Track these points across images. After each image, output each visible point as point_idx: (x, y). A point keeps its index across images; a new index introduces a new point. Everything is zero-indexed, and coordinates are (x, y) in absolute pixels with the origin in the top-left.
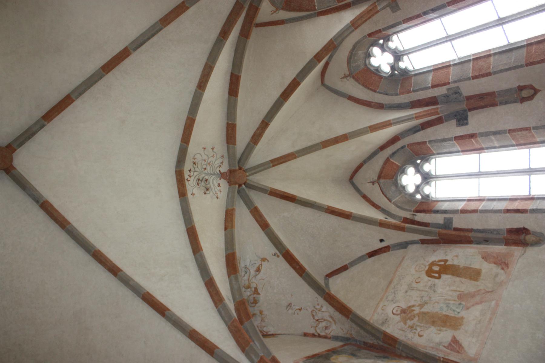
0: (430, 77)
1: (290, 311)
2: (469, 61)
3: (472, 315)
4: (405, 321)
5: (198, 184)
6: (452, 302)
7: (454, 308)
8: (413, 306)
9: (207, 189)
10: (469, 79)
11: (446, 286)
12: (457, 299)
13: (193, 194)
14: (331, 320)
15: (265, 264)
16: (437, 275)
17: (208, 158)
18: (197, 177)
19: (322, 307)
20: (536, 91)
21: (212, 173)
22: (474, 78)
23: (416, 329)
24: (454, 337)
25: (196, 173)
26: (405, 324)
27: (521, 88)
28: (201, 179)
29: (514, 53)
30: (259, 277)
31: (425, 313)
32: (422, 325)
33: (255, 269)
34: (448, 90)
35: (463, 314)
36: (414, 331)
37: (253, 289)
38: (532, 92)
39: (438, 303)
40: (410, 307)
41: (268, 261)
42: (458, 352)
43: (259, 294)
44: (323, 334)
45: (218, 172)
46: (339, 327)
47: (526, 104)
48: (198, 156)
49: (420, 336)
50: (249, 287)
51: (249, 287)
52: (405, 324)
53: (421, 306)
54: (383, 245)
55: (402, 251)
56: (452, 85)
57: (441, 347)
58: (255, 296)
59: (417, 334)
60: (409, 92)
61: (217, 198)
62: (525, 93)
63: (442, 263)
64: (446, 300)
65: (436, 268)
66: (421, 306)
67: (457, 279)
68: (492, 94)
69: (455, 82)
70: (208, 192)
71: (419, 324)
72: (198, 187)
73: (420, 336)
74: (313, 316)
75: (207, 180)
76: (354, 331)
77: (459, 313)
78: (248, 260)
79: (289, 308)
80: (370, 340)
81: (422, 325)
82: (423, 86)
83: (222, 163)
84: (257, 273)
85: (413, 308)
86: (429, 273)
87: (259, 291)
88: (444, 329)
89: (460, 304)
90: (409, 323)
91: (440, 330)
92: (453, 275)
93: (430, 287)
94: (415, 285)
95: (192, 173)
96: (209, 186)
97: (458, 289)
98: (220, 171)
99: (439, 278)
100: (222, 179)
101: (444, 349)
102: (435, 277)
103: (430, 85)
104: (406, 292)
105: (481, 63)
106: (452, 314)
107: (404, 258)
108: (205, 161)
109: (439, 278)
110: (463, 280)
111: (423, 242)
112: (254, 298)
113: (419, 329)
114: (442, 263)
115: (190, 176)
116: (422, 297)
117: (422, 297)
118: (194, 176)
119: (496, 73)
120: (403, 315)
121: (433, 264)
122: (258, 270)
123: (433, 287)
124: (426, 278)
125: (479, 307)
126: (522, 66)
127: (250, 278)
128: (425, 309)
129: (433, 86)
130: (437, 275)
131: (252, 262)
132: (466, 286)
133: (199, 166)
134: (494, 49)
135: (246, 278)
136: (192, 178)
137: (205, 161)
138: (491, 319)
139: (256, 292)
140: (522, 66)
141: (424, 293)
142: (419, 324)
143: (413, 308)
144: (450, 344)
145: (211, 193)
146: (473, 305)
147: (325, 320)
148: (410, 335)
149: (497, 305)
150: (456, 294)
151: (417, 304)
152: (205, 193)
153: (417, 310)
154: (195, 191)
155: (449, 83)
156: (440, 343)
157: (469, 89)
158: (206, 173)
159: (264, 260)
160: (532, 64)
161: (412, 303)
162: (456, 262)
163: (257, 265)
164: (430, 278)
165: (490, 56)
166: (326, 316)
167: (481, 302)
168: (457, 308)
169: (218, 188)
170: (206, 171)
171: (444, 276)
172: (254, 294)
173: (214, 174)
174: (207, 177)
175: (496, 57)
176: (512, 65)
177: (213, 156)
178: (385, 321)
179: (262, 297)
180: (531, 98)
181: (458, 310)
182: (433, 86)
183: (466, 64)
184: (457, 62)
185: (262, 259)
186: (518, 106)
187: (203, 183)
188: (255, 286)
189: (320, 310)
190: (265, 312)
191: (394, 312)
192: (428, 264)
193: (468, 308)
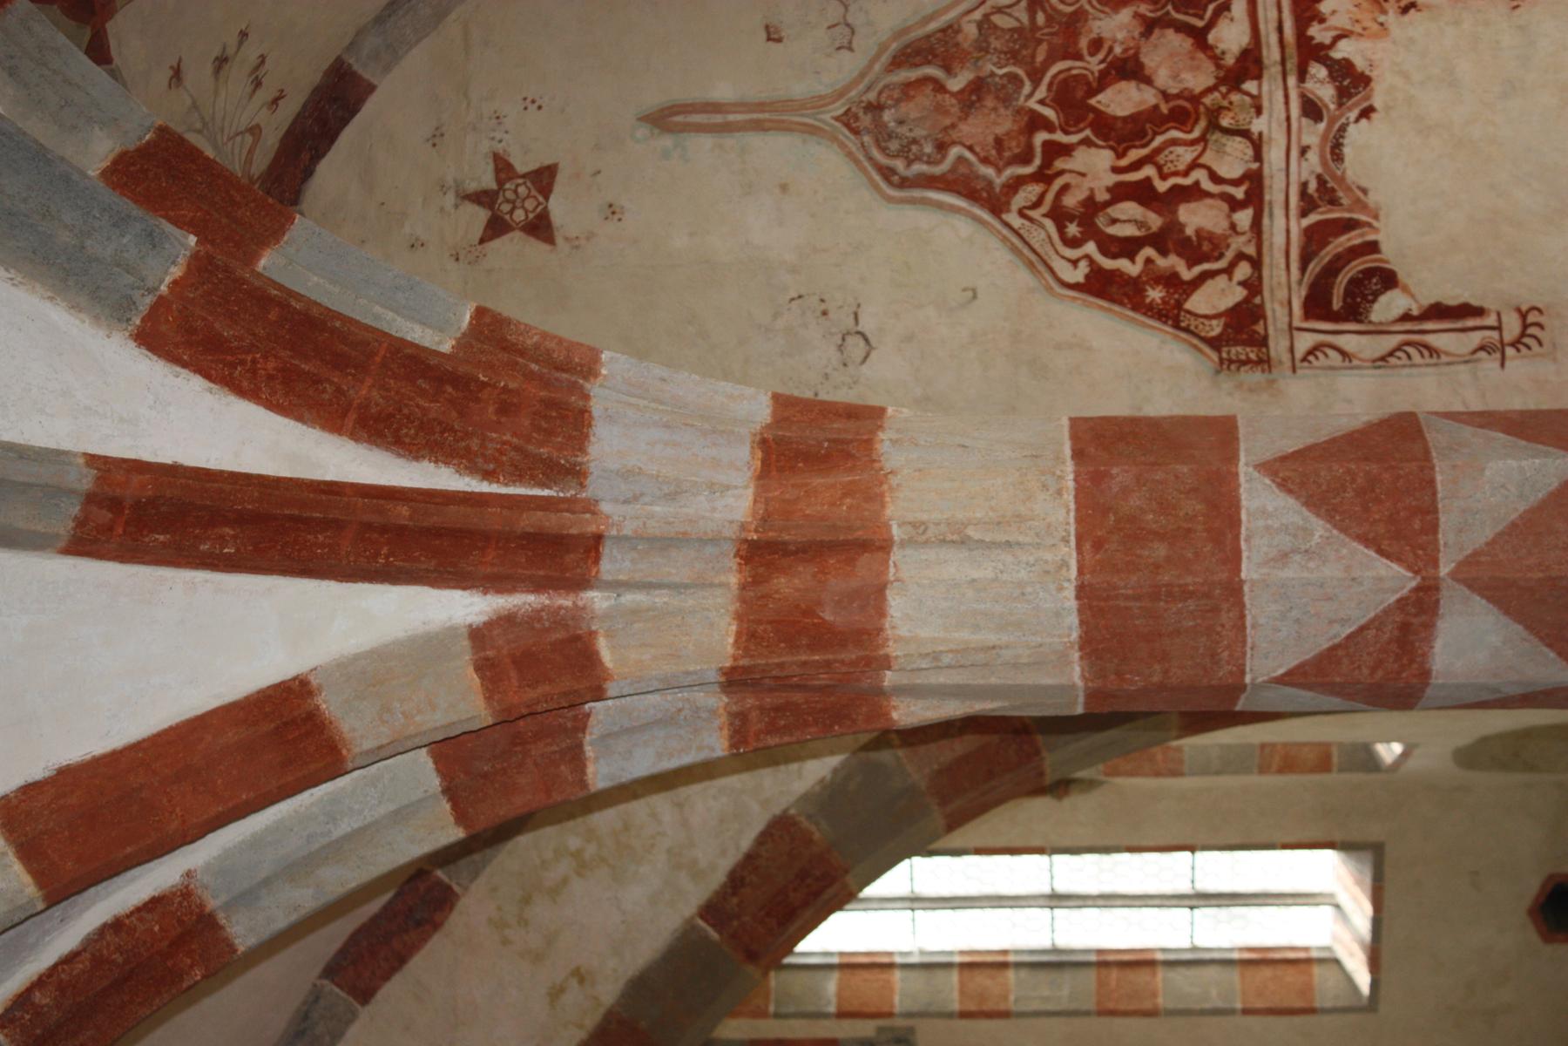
0: (831, 985)
2: (948, 966)
10: (950, 1015)
22: (964, 1015)
29: (1067, 977)
34: (880, 1030)
56: (899, 1022)
60: (761, 1014)
69: (909, 1015)
82: (811, 1008)
103: (832, 1009)
105: (981, 979)
126: (1087, 1013)
129: (842, 1015)
134: (1017, 952)
140: (1087, 1013)
155: (890, 1015)
160: (1113, 1013)
165: (1004, 965)
175: (1023, 973)
176: (1065, 1005)
182: (842, 1015)
183: (940, 974)
184: (915, 959)
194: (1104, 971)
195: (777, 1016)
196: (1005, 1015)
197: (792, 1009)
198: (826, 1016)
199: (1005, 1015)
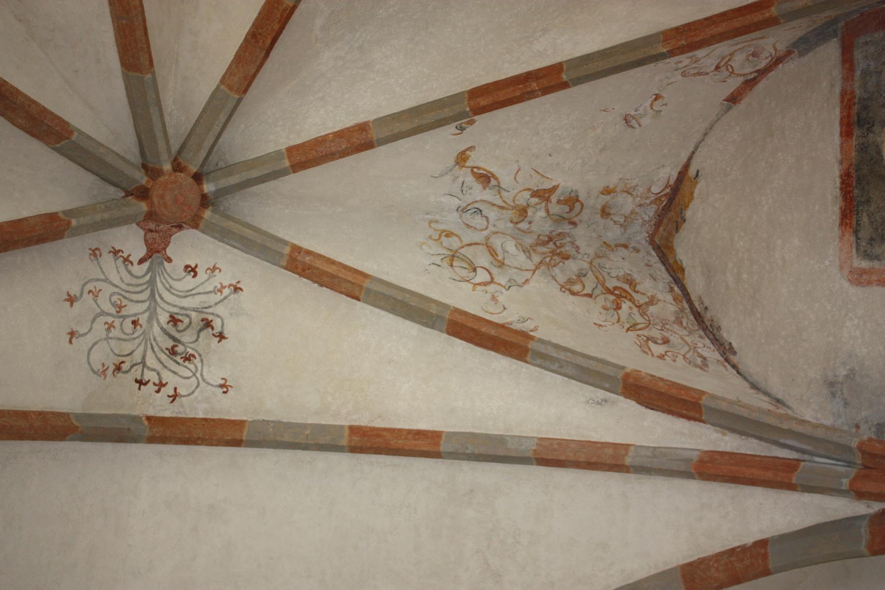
5: (188, 358)
9: (208, 324)
15: (476, 159)
17: (103, 313)
18: (163, 357)
21: (145, 295)
25: (151, 361)
28: (170, 343)
30: (506, 180)
33: (478, 187)
37: (536, 200)
41: (471, 148)
50: (523, 212)
51: (523, 212)
58: (554, 199)
61: (237, 289)
70: (217, 324)
72: (197, 361)
75: (174, 320)
78: (445, 200)
84: (493, 182)
95: (149, 375)
96: (193, 314)
98: (141, 262)
100: (169, 252)
108: (110, 326)
112: (559, 202)
115: (161, 385)
118: (158, 367)
122: (485, 178)
127: (500, 202)
131: (456, 190)
135: (492, 214)
136: (166, 376)
137: (110, 326)
139: (543, 195)
145: (220, 310)
152: (221, 336)
158: (150, 320)
159: (462, 159)
163: (470, 179)
169: (202, 275)
170: (143, 319)
172: (548, 200)
173: (152, 283)
174: (164, 318)
177: (95, 294)
179: (565, 181)
185: (457, 163)
187: (187, 337)
188: (527, 195)
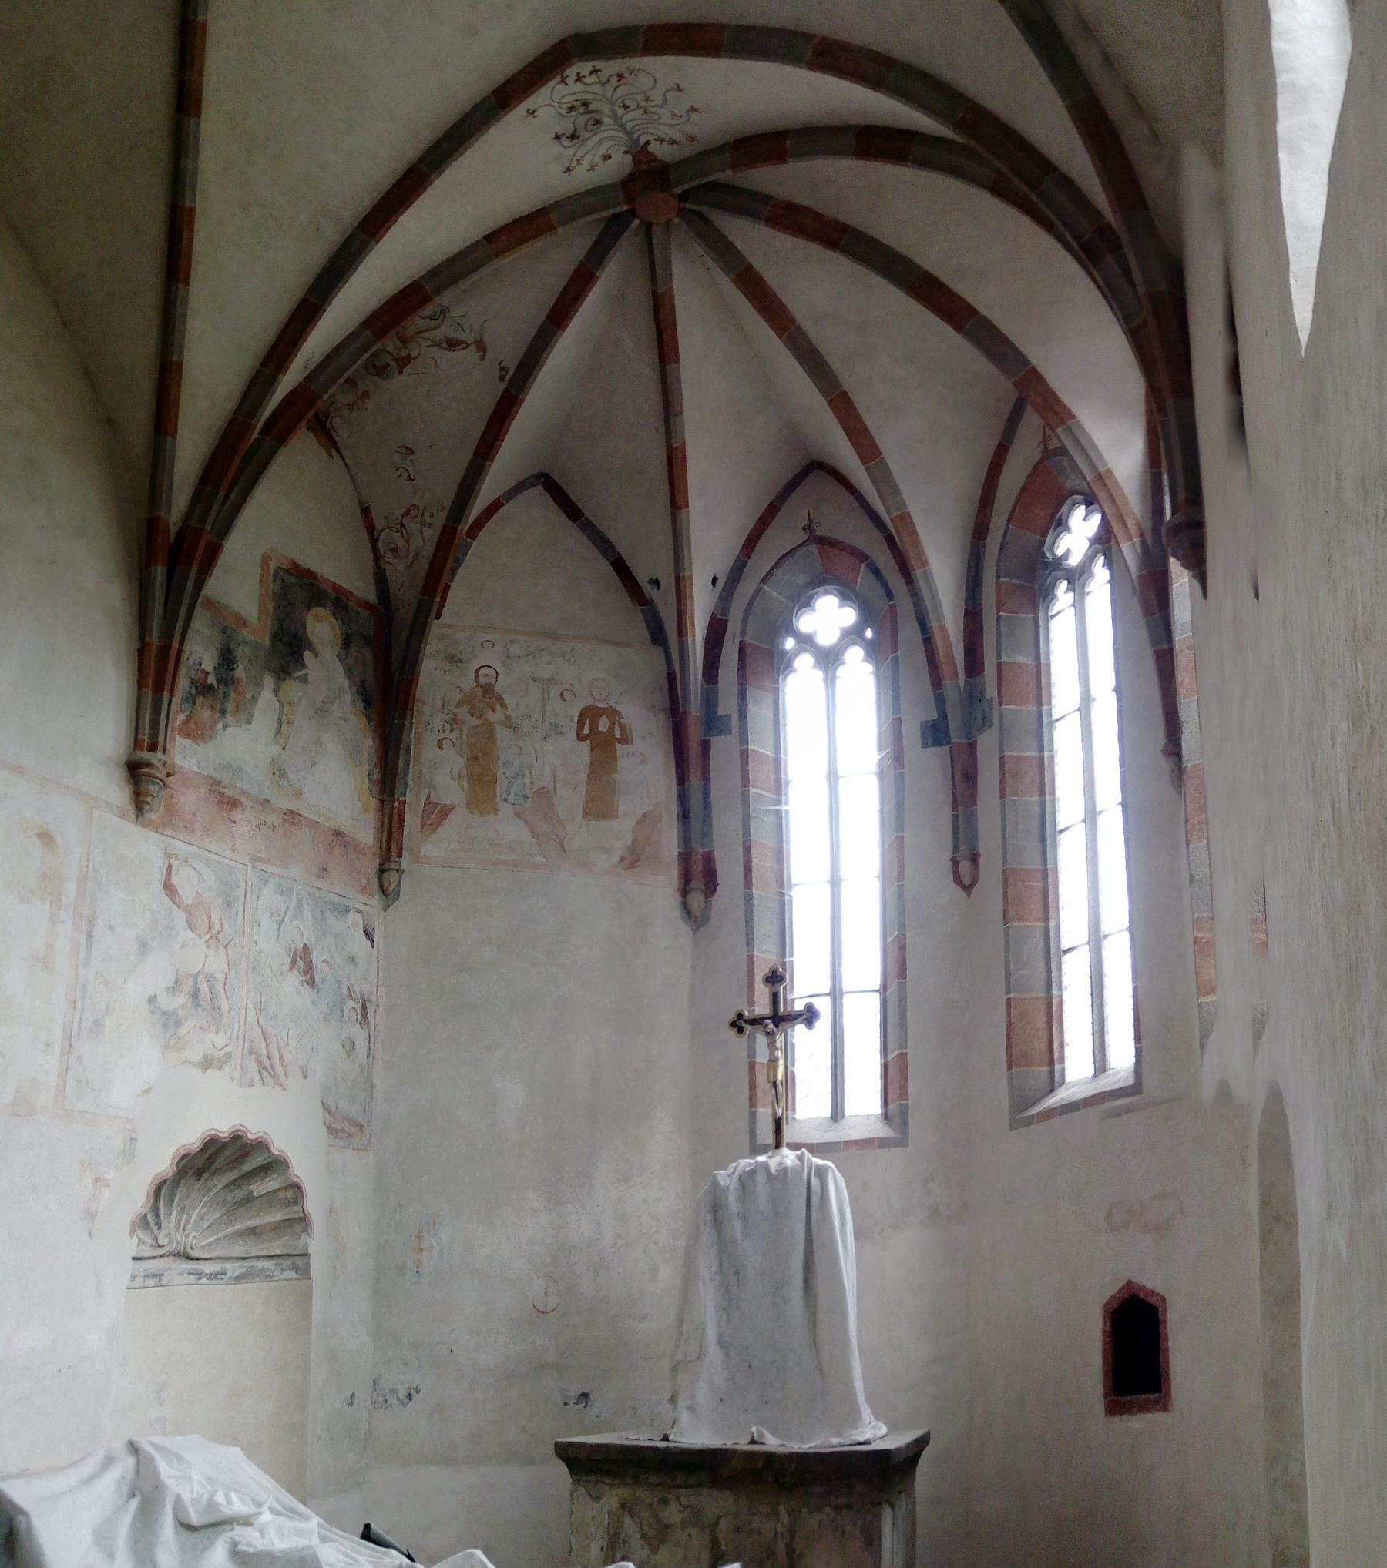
1: (397, 458)
3: (507, 827)
4: (467, 700)
5: (571, 109)
6: (527, 781)
7: (514, 788)
8: (504, 706)
9: (573, 137)
11: (562, 759)
12: (538, 785)
13: (531, 113)
14: (412, 555)
15: (472, 353)
16: (586, 731)
17: (660, 106)
18: (590, 96)
19: (430, 525)
20: (968, 888)
21: (630, 125)
23: (452, 730)
24: (452, 808)
25: (597, 88)
26: (460, 704)
27: (974, 858)
28: (591, 107)
30: (436, 352)
31: (491, 734)
32: (464, 738)
33: (452, 335)
35: (505, 810)
36: (448, 727)
37: (404, 353)
38: (967, 881)
39: (520, 753)
40: (500, 699)
41: (482, 358)
42: (423, 825)
43: (400, 371)
44: (381, 547)
45: (642, 141)
46: (404, 577)
47: (948, 867)
48: (645, 81)
49: (440, 745)
50: (404, 341)
51: (404, 341)
52: (460, 704)
53: (509, 723)
54: (648, 589)
55: (646, 634)
57: (427, 790)
58: (393, 364)
59: (442, 736)
61: (568, 170)
62: (965, 866)
63: (618, 734)
64: (531, 766)
65: (603, 725)
66: (509, 723)
67: (583, 776)
68: (972, 799)
70: (566, 142)
71: (465, 732)
72: (563, 112)
73: (440, 745)
74: (407, 513)
75: (598, 122)
76: (404, 614)
77: (506, 800)
78: (463, 310)
79: (403, 450)
80: (396, 653)
81: (464, 738)
83: (674, 142)
84: (445, 345)
85: (498, 708)
86: (589, 714)
87: (407, 370)
88: (466, 785)
89: (525, 797)
90: (464, 712)
91: (461, 777)
92: (592, 764)
93: (556, 726)
94: (555, 691)
95: (594, 78)
96: (588, 135)
97: (558, 785)
98: (648, 143)
99: (581, 738)
100: (630, 157)
101: (424, 798)
102: (580, 727)
104: (535, 680)
106: (500, 789)
107: (627, 645)
108: (647, 99)
109: (581, 738)
110: (583, 788)
111: (671, 677)
112: (388, 364)
113: (453, 736)
114: (618, 734)
115: (579, 79)
116: (528, 716)
117: (528, 716)
118: (589, 89)
119: (1003, 807)
120: (479, 691)
121: (613, 714)
122: (453, 344)
123: (557, 730)
124: (575, 712)
125: (526, 835)
127: (426, 334)
128: (501, 733)
130: (586, 731)
131: (462, 321)
132: (570, 799)
133: (621, 91)
135: (422, 324)
136: (579, 87)
137: (647, 99)
138: (504, 863)
139: (403, 362)
141: (539, 717)
142: (465, 732)
143: (498, 708)
144: (436, 805)
145: (570, 151)
146: (526, 823)
147: (407, 541)
148: (437, 723)
149: (536, 867)
150: (547, 782)
151: (509, 713)
152: (558, 137)
153: (496, 717)
154: (545, 114)
156: (432, 786)
157: (987, 743)
158: (615, 113)
159: (481, 347)
161: (510, 701)
162: (622, 763)
163: (462, 337)
164: (576, 718)
166: (417, 542)
167: (535, 835)
168: (516, 794)
169: (598, 159)
170: (621, 111)
171: (585, 746)
172: (396, 360)
173: (630, 134)
174: (606, 120)
178: (453, 660)
180: (957, 879)
181: (511, 799)
185: (481, 341)
186: (948, 854)
187: (582, 120)
188: (414, 353)
189: (422, 524)
190: (370, 405)
191: (482, 671)
192: (611, 703)
193: (518, 815)
194: (1039, 875)
195: (998, 618)
196: (1003, 796)
197: (1003, 629)
198: (999, 656)
199: (1003, 796)
